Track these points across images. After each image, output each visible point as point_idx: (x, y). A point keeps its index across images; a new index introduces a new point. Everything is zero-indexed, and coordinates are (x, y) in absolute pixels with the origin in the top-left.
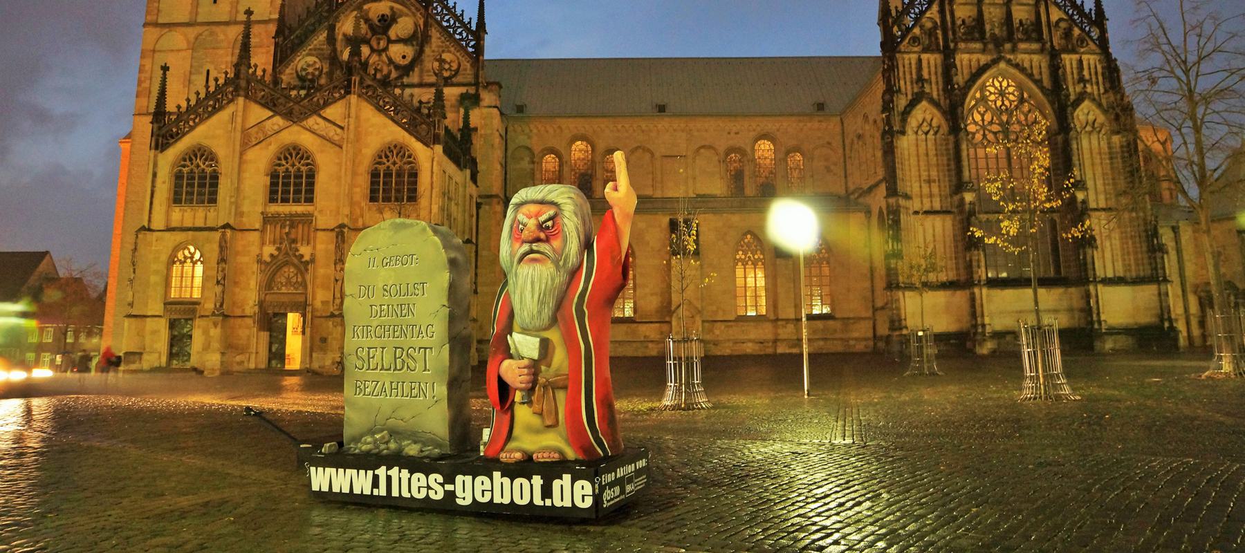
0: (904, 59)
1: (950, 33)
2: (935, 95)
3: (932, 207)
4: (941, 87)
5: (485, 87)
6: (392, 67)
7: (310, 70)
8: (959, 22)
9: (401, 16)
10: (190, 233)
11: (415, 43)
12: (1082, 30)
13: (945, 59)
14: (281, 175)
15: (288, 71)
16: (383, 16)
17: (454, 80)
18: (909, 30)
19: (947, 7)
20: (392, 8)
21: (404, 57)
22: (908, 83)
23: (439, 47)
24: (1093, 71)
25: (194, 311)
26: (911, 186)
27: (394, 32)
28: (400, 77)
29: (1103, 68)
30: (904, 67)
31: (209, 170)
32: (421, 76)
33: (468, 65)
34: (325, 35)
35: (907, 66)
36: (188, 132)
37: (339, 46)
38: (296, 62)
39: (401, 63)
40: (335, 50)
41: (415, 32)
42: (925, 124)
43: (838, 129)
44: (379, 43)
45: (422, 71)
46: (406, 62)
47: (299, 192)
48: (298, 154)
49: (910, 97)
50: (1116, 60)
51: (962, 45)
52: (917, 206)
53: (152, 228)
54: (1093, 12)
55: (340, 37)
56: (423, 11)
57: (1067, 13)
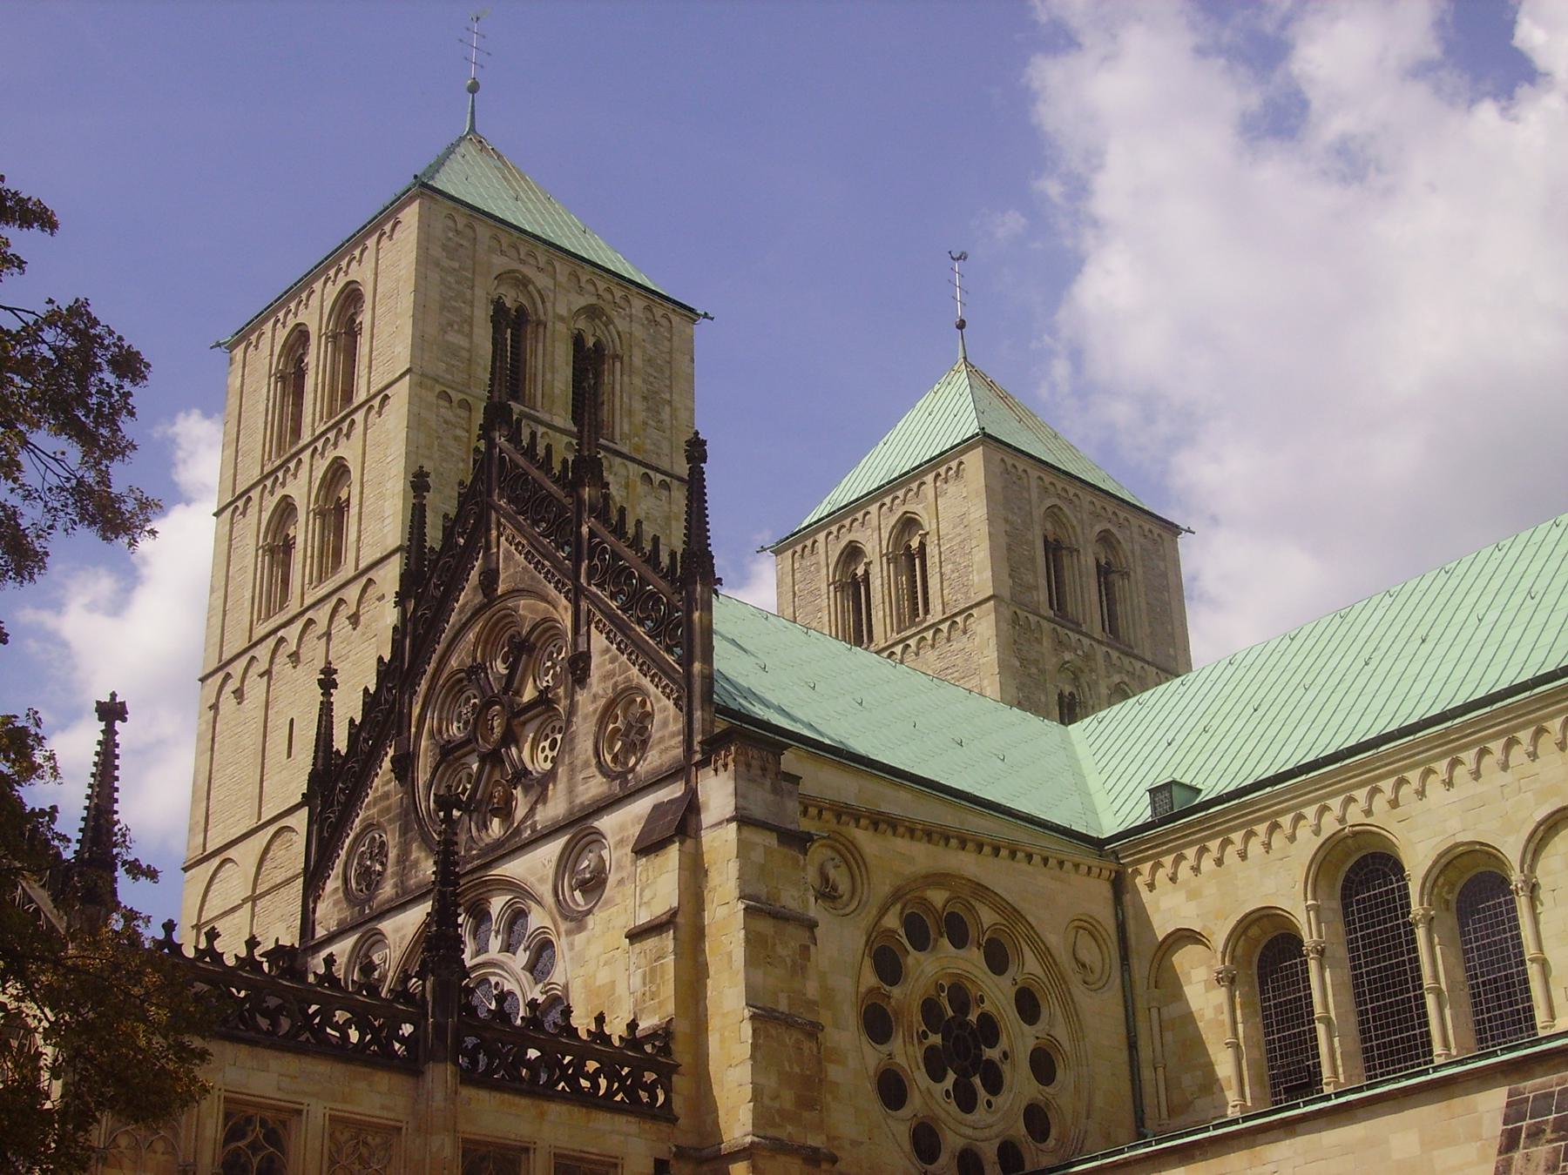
5: (704, 763)
28: (532, 811)
32: (571, 791)
38: (343, 853)
45: (572, 771)
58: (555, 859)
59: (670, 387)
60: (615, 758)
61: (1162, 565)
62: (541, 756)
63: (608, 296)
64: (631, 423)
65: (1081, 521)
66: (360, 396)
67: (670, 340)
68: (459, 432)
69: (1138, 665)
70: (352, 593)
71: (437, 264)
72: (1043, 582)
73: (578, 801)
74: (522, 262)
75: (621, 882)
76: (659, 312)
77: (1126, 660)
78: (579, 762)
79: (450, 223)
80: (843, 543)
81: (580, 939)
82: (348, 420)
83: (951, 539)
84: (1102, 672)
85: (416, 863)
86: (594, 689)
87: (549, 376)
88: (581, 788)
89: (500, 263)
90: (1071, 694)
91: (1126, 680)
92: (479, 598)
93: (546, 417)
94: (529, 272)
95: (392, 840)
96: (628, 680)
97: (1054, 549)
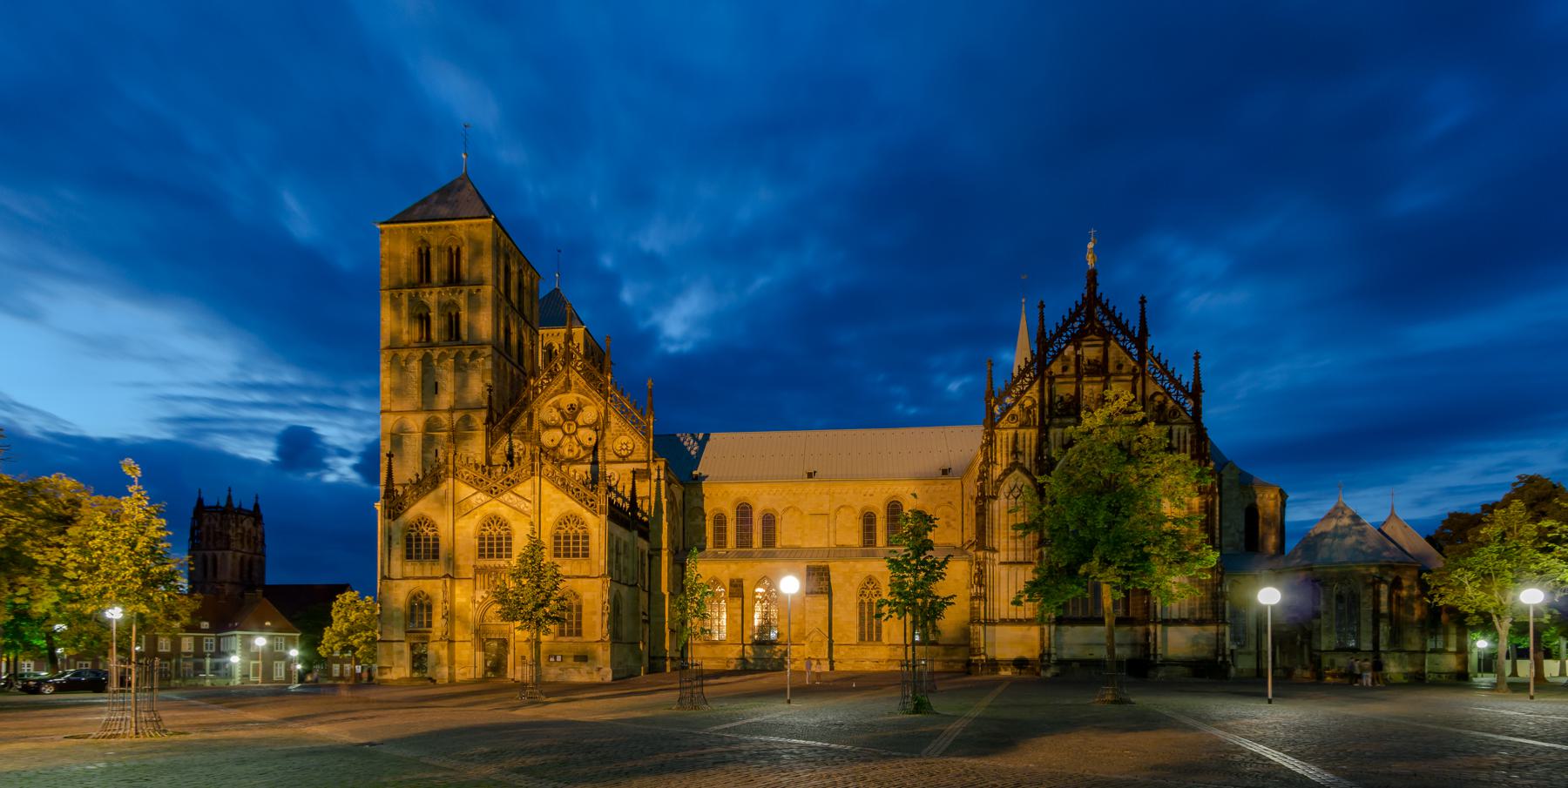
0: (1002, 434)
1: (1047, 410)
2: (1027, 466)
3: (1016, 559)
4: (1033, 457)
6: (581, 448)
8: (1057, 399)
9: (585, 405)
10: (421, 581)
12: (1177, 402)
13: (1040, 432)
14: (495, 537)
16: (572, 405)
17: (630, 458)
18: (1009, 407)
19: (1046, 387)
20: (578, 399)
21: (590, 439)
22: (1004, 455)
23: (617, 431)
24: (1182, 440)
25: (428, 638)
26: (999, 543)
29: (1192, 437)
30: (1001, 441)
31: (431, 534)
34: (526, 421)
35: (1004, 440)
36: (413, 505)
41: (598, 419)
42: (1016, 490)
43: (959, 491)
46: (593, 443)
47: (501, 550)
48: (498, 521)
49: (1004, 467)
50: (1206, 429)
51: (1057, 421)
52: (1003, 559)
53: (392, 577)
54: (1190, 385)
56: (603, 400)
57: (1163, 387)
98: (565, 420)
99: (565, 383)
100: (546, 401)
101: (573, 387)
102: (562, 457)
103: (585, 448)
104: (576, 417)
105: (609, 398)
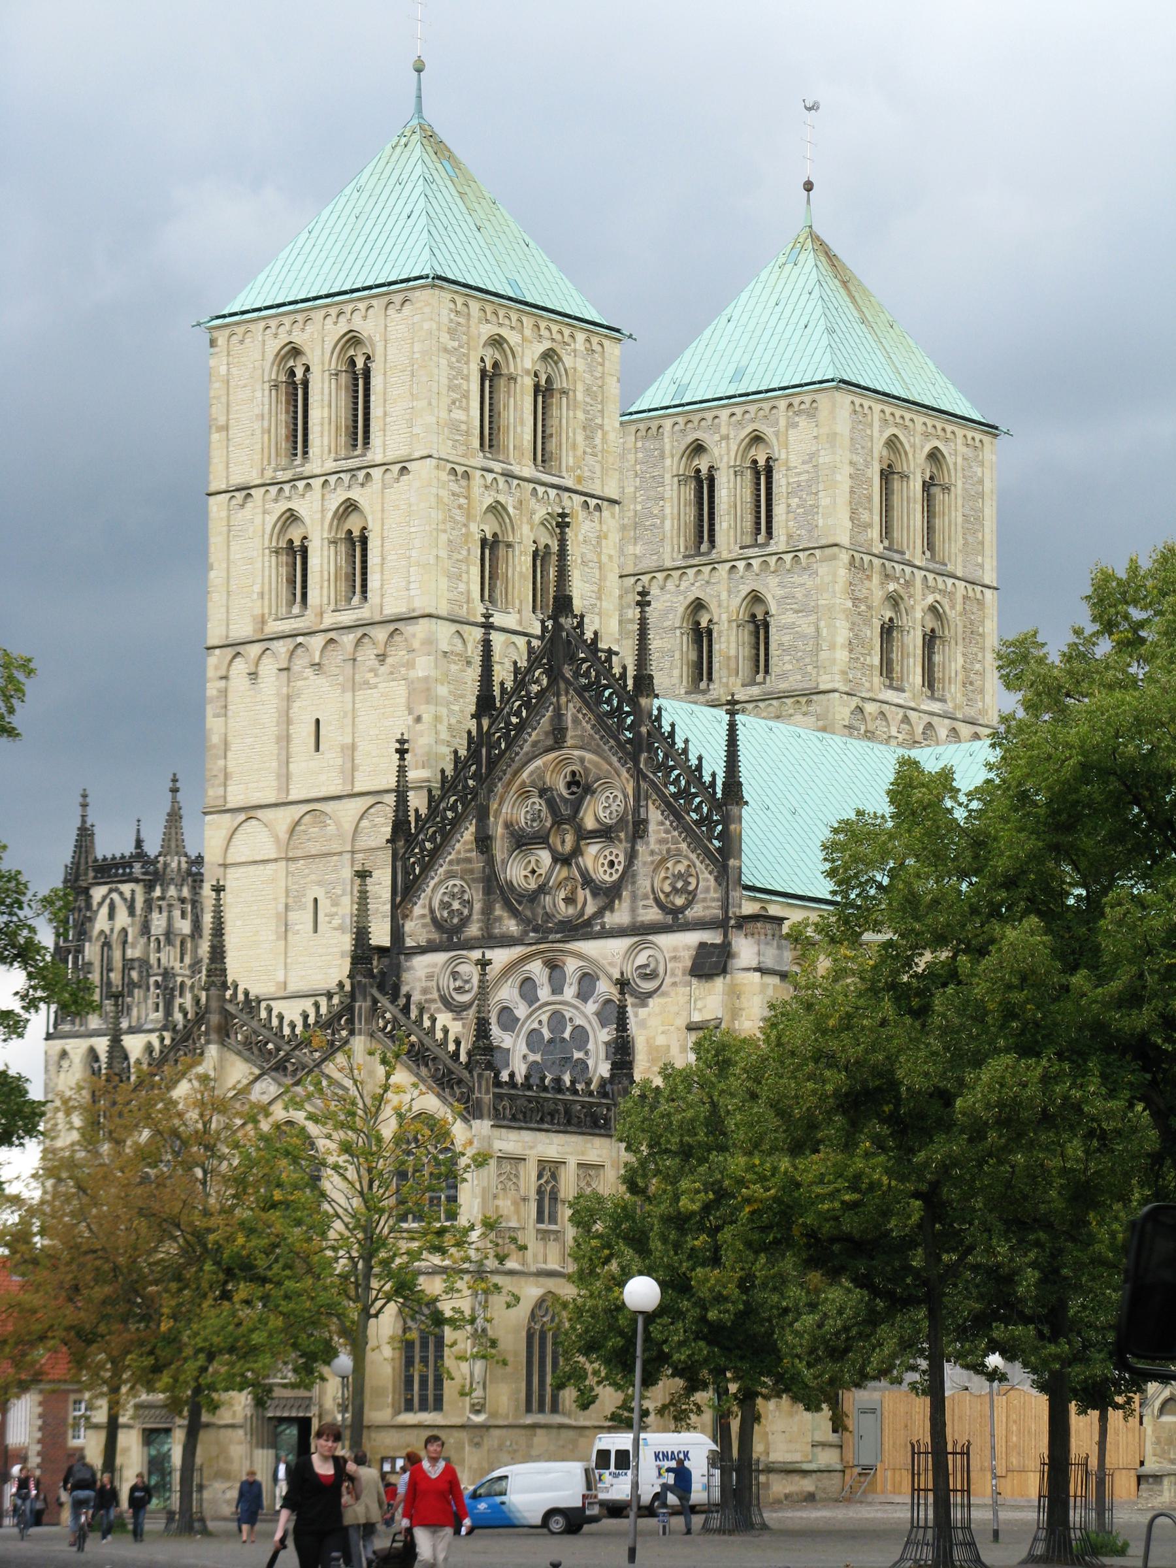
5: (739, 927)
6: (587, 891)
7: (456, 905)
11: (622, 835)
15: (418, 910)
16: (573, 773)
20: (582, 760)
21: (612, 864)
23: (661, 841)
27: (594, 813)
28: (600, 913)
32: (633, 910)
33: (712, 878)
34: (472, 829)
37: (500, 848)
38: (429, 890)
39: (607, 878)
40: (490, 861)
44: (563, 842)
45: (634, 897)
55: (499, 831)
58: (622, 952)
59: (602, 411)
60: (667, 895)
61: (979, 471)
62: (601, 870)
63: (558, 337)
64: (575, 456)
65: (913, 446)
66: (376, 454)
67: (602, 365)
68: (462, 501)
69: (950, 581)
70: (380, 634)
71: (446, 350)
72: (877, 518)
73: (640, 919)
74: (500, 325)
75: (674, 984)
76: (595, 340)
77: (940, 579)
78: (640, 892)
79: (452, 306)
80: (690, 439)
81: (643, 1012)
82: (364, 472)
83: (799, 474)
84: (919, 597)
85: (499, 919)
86: (653, 846)
87: (519, 429)
88: (641, 911)
89: (487, 330)
90: (891, 620)
91: (938, 598)
92: (550, 742)
93: (516, 469)
94: (504, 332)
95: (476, 895)
96: (678, 849)
97: (887, 475)
98: (558, 821)
99: (552, 719)
100: (517, 773)
101: (570, 733)
102: (548, 916)
103: (596, 889)
104: (577, 810)
105: (644, 755)
